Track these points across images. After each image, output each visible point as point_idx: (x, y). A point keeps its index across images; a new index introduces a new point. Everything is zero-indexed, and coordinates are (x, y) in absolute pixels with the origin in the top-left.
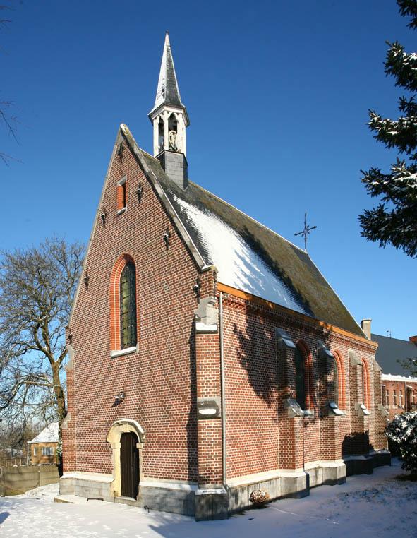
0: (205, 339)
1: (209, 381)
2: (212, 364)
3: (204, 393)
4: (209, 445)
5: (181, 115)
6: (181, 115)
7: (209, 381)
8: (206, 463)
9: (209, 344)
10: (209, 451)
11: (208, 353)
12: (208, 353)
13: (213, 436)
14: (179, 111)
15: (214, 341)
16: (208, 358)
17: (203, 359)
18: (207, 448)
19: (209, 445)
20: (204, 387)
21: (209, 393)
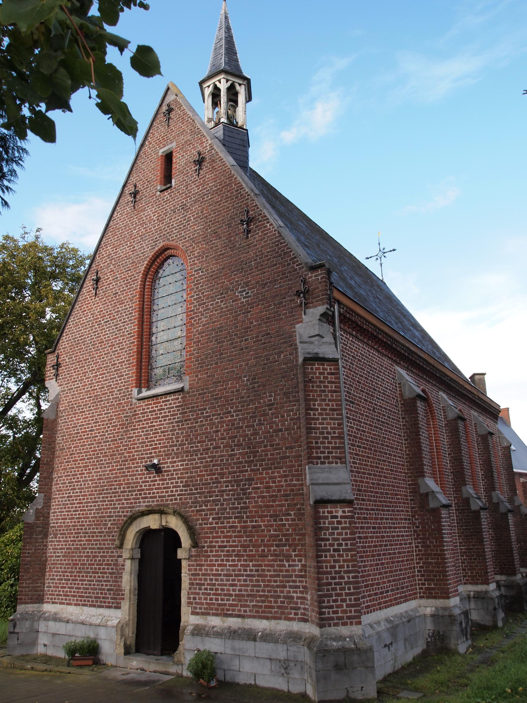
0: (319, 369)
1: (327, 438)
2: (331, 410)
3: (320, 458)
4: (335, 550)
5: (243, 87)
6: (243, 87)
7: (327, 438)
8: (330, 584)
9: (324, 378)
10: (335, 561)
11: (325, 391)
12: (325, 391)
13: (341, 534)
14: (241, 82)
15: (332, 374)
16: (324, 400)
17: (316, 400)
18: (333, 556)
19: (335, 550)
20: (319, 448)
21: (328, 457)
